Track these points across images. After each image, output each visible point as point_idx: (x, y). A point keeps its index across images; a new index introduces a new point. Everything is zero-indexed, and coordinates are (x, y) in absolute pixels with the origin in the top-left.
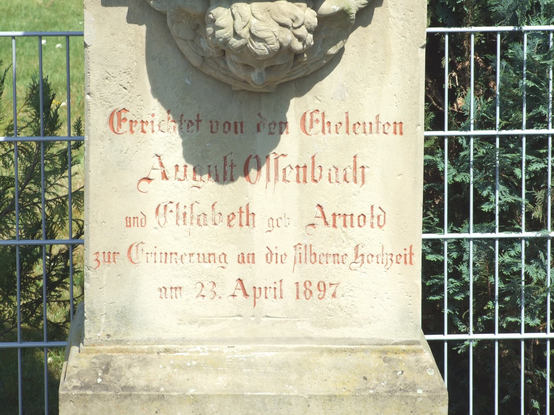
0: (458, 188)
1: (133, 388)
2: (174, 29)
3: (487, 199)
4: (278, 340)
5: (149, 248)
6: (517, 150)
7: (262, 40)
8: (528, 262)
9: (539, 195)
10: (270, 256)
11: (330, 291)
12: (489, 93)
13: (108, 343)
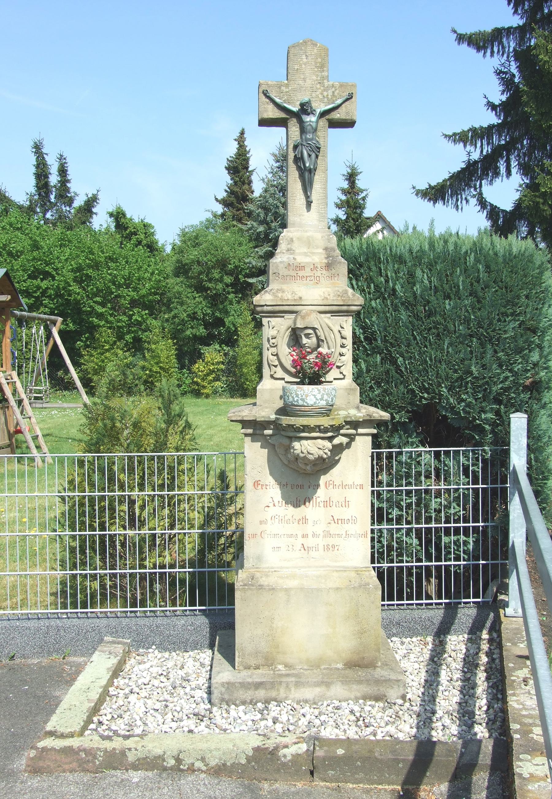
0: (380, 509)
1: (263, 585)
2: (278, 450)
3: (391, 513)
4: (317, 567)
5: (268, 532)
6: (401, 495)
7: (312, 454)
8: (406, 537)
9: (410, 512)
10: (314, 535)
11: (336, 548)
12: (390, 474)
13: (253, 568)
